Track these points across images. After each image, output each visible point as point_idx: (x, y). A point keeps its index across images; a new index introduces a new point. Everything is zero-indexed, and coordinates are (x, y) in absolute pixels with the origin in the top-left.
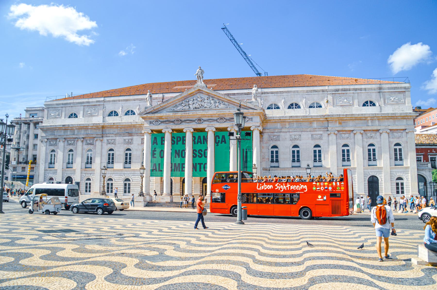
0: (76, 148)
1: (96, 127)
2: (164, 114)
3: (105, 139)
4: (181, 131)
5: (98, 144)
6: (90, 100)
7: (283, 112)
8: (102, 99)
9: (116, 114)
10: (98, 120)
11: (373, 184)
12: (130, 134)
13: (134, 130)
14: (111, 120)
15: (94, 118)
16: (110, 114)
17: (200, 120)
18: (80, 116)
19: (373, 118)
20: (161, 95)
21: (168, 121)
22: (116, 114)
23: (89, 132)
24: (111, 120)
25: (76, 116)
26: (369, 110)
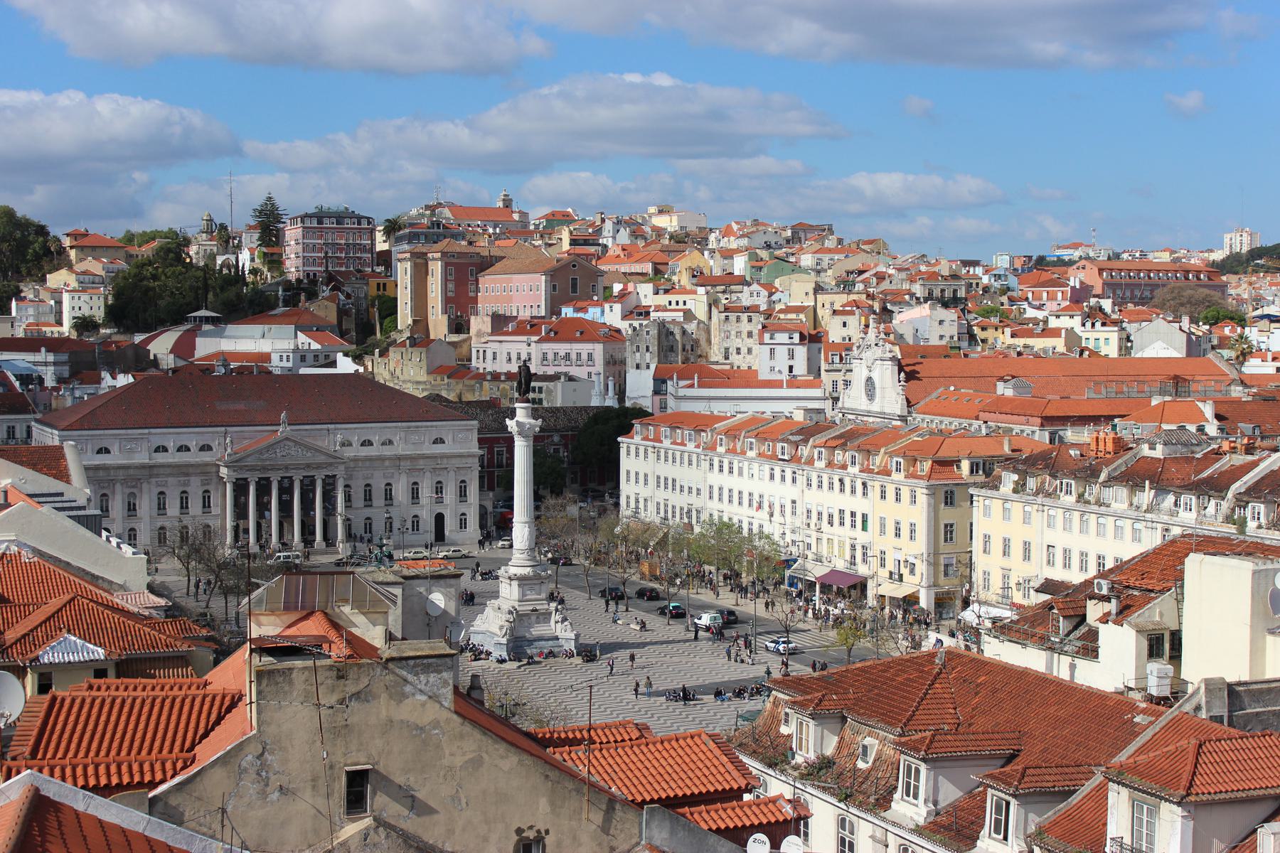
0: (114, 493)
1: (143, 467)
2: (250, 462)
3: (153, 480)
4: (268, 479)
5: (145, 486)
6: (130, 431)
7: (356, 451)
8: (146, 431)
9: (165, 449)
10: (142, 458)
11: (440, 519)
12: (187, 475)
13: (191, 470)
14: (161, 458)
15: (137, 455)
16: (157, 450)
17: (287, 468)
18: (115, 449)
19: (443, 456)
20: (223, 429)
21: (252, 469)
22: (165, 449)
23: (131, 472)
24: (161, 458)
25: (107, 451)
26: (439, 449)
